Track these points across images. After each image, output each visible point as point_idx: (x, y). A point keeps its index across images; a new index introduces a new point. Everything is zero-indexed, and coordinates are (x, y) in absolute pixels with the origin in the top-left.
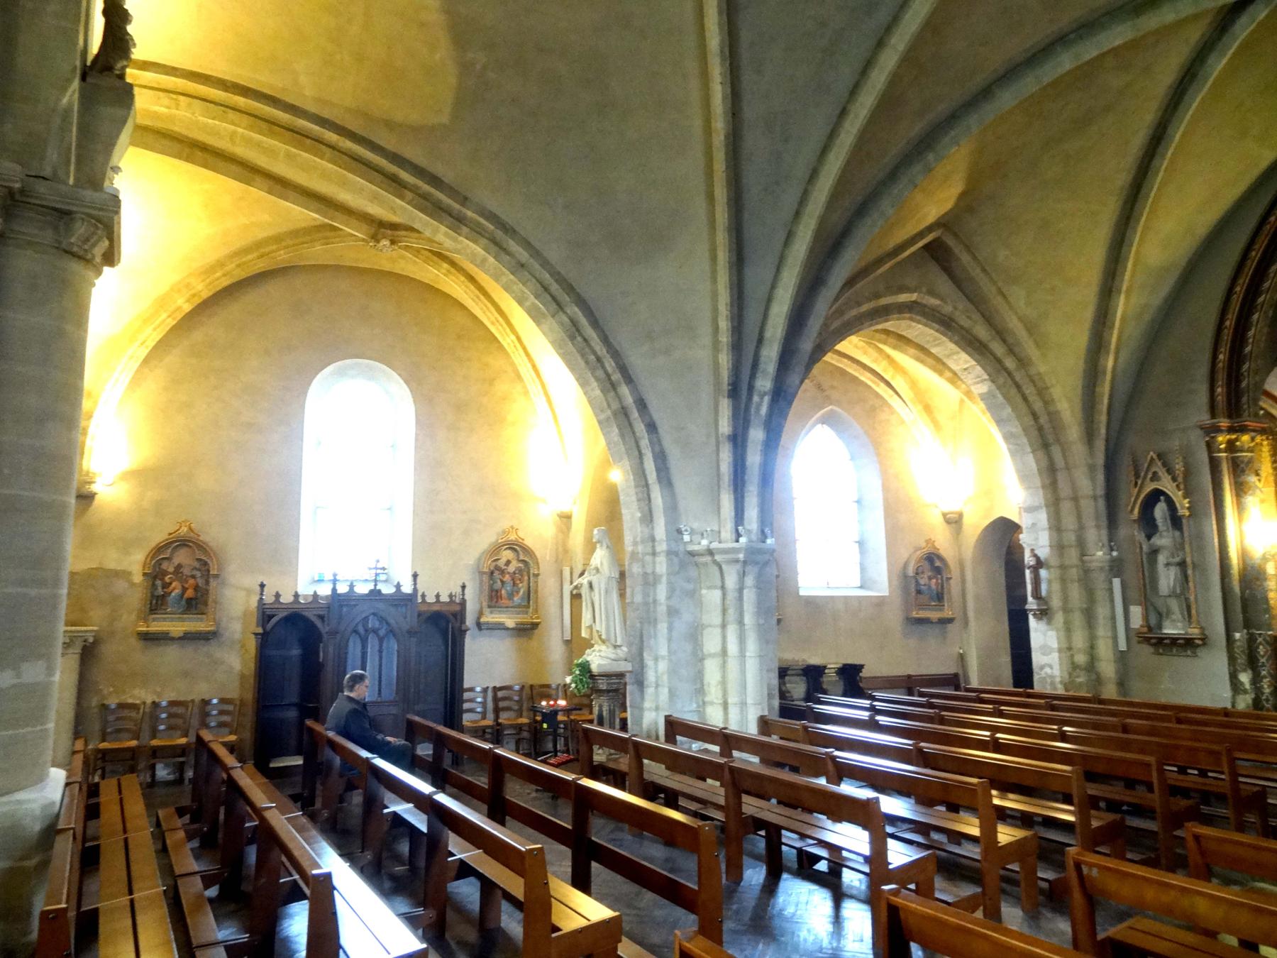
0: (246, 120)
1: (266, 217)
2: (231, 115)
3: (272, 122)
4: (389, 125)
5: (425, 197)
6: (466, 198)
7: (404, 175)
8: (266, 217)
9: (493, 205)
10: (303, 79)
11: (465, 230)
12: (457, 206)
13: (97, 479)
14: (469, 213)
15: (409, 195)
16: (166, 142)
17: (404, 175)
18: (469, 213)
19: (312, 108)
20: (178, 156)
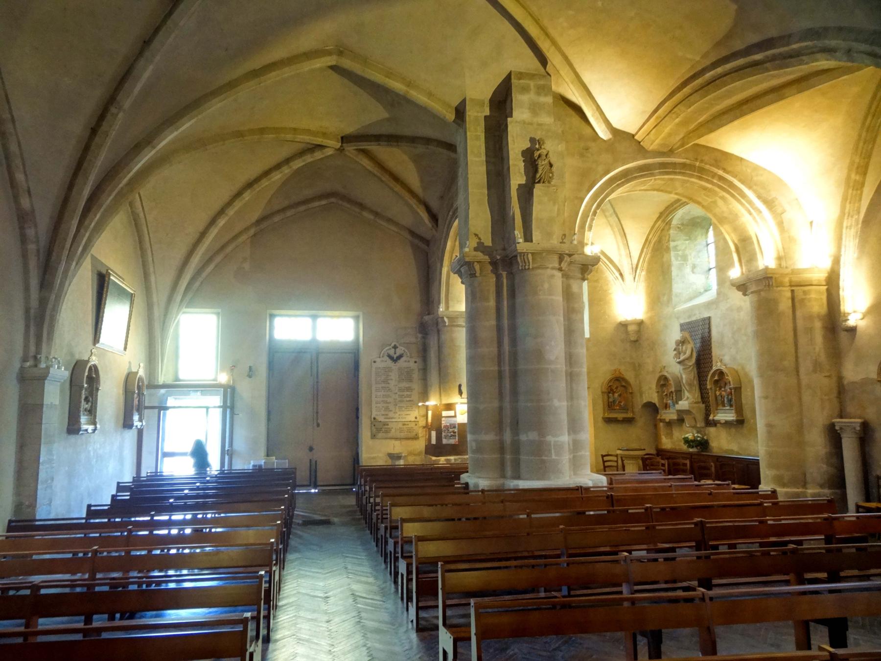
0: (696, 96)
1: (855, 90)
2: (692, 98)
3: (702, 87)
4: (729, 36)
5: (773, 58)
6: (790, 36)
7: (758, 57)
8: (855, 90)
9: (805, 23)
10: (690, 56)
11: (804, 58)
12: (786, 49)
13: (849, 317)
14: (795, 46)
15: (768, 65)
16: (726, 116)
17: (758, 57)
18: (795, 46)
19: (707, 62)
20: (736, 118)
